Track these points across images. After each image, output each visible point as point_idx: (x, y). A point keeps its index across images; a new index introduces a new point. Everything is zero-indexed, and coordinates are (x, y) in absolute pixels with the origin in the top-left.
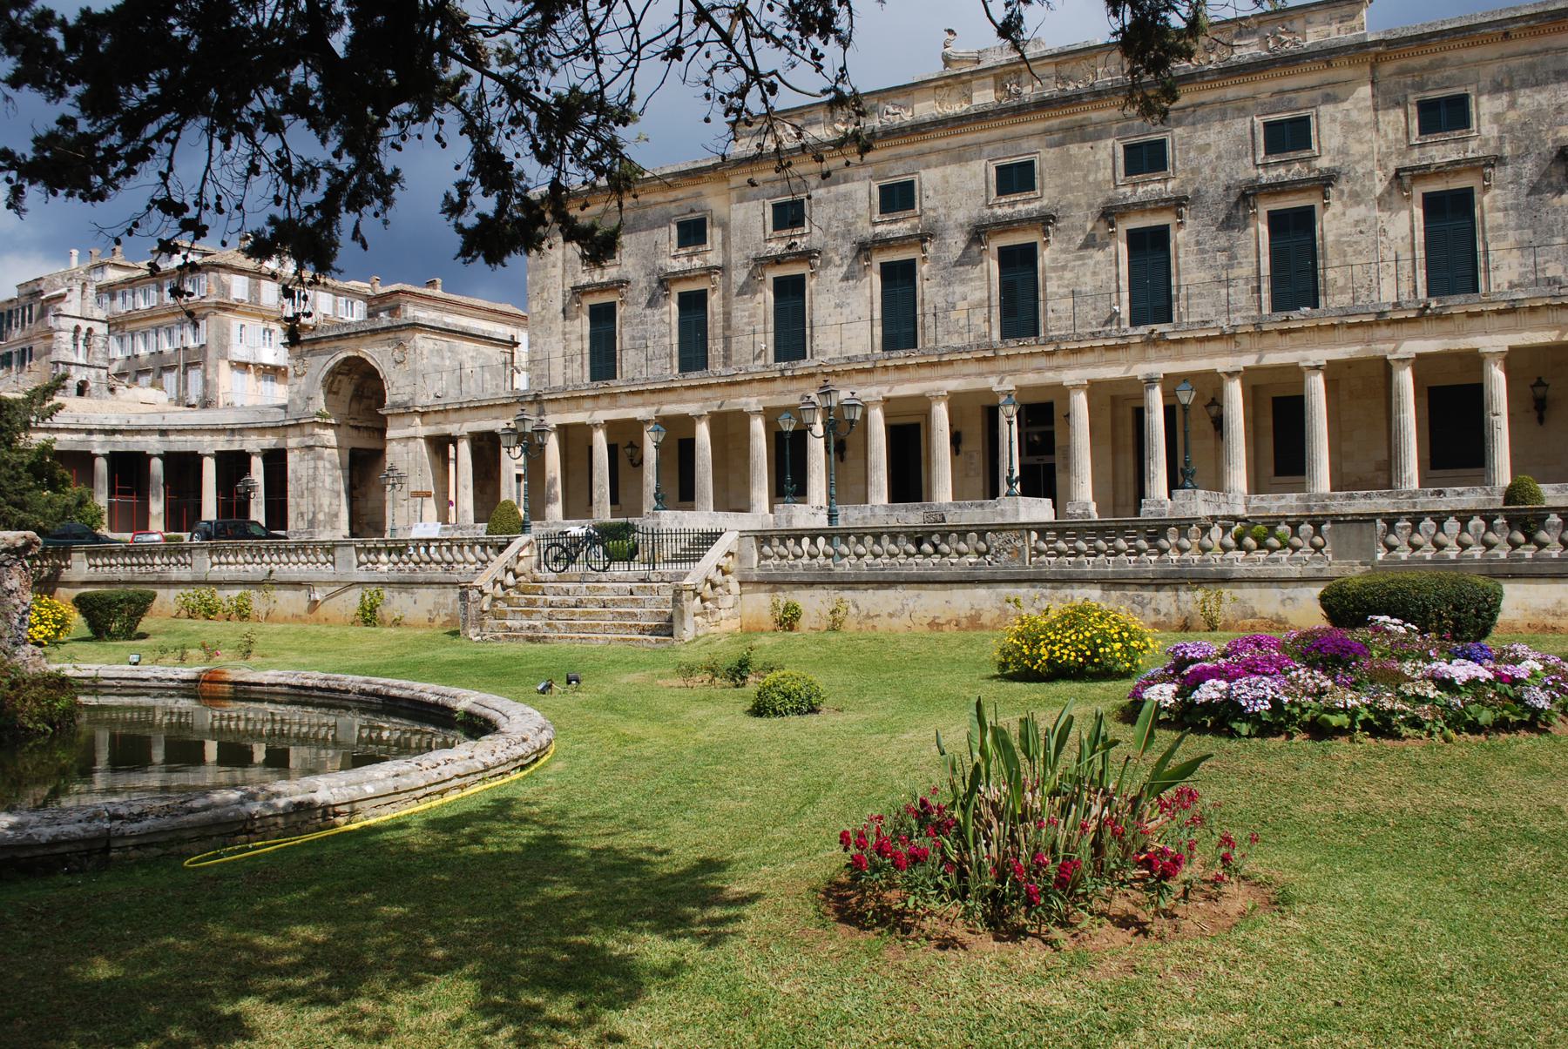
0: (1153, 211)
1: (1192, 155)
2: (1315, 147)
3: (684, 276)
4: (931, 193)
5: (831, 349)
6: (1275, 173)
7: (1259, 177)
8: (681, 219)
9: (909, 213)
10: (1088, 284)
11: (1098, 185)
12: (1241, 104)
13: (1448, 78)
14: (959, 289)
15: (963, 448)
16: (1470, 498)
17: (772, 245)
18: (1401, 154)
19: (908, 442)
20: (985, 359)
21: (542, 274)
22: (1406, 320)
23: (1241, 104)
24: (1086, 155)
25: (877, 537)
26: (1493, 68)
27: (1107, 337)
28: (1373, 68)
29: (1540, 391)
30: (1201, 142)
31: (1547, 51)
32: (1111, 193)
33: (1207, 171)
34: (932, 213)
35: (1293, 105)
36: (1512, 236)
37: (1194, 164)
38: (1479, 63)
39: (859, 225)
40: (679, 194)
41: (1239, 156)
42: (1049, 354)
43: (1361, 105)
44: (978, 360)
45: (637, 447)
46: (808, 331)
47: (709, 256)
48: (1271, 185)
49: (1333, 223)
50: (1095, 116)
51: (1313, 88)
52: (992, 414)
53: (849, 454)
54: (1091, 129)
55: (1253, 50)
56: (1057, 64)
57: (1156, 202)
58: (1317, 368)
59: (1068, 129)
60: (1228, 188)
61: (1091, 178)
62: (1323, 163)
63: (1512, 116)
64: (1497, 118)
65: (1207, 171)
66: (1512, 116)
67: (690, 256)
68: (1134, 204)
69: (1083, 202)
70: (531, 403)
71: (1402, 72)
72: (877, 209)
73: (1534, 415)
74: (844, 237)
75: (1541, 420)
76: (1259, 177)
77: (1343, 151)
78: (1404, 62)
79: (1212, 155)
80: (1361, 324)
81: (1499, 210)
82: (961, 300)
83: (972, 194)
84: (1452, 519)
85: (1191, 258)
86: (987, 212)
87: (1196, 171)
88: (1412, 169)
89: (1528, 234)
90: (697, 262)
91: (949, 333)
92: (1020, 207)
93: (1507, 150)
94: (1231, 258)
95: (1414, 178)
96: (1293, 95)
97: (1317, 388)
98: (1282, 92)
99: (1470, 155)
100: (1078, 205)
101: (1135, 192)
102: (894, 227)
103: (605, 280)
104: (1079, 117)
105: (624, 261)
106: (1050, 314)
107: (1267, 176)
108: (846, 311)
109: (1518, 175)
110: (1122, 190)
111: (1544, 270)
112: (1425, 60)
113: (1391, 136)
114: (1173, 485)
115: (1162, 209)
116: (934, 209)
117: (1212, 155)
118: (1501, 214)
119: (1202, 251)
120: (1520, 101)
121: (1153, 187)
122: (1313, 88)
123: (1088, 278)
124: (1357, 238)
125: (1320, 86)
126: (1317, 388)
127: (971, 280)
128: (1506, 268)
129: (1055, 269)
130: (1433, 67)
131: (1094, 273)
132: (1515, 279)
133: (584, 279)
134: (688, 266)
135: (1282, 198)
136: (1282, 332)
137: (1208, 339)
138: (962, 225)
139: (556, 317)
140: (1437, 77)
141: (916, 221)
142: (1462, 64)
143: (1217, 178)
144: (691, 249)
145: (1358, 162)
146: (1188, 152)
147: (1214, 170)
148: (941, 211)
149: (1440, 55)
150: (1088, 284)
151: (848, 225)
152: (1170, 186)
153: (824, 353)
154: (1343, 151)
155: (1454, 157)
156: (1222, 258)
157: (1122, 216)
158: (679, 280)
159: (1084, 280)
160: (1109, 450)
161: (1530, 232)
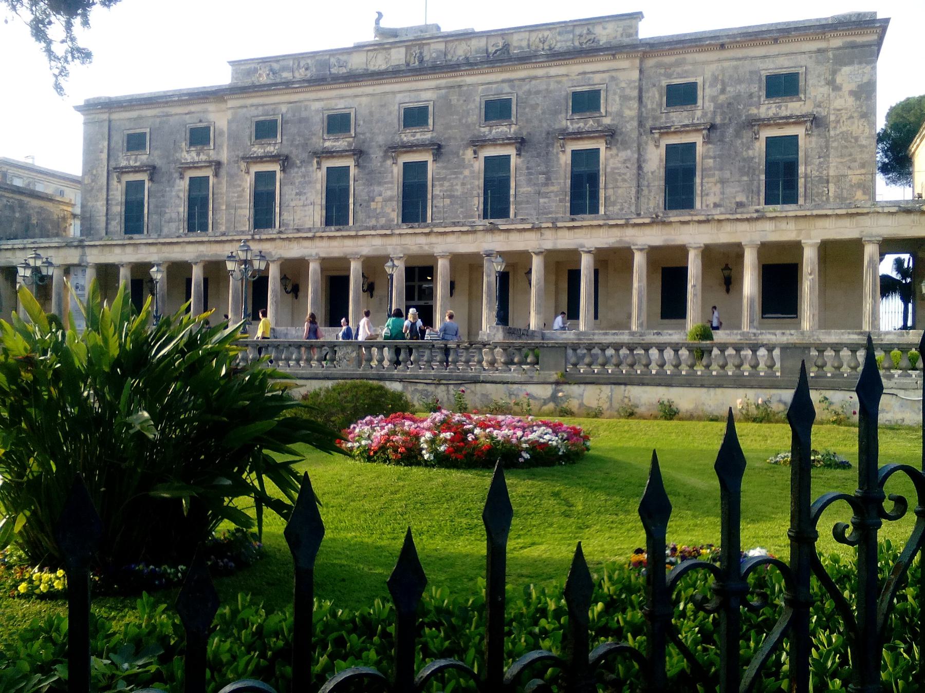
0: (501, 145)
1: (527, 110)
2: (603, 110)
3: (194, 166)
4: (361, 123)
6: (577, 126)
7: (567, 128)
8: (192, 126)
10: (459, 190)
11: (468, 126)
12: (559, 79)
13: (686, 71)
14: (377, 189)
16: (674, 336)
20: (386, 235)
22: (644, 224)
23: (559, 79)
26: (713, 67)
27: (463, 225)
28: (641, 62)
29: (727, 272)
30: (533, 102)
31: (745, 58)
32: (476, 132)
34: (362, 137)
35: (591, 82)
38: (704, 63)
39: (314, 139)
40: (193, 108)
41: (556, 113)
42: (426, 234)
43: (632, 85)
44: (381, 235)
46: (277, 210)
48: (574, 133)
50: (469, 80)
51: (604, 72)
54: (465, 88)
55: (569, 44)
56: (446, 42)
57: (503, 139)
58: (589, 252)
59: (452, 87)
60: (548, 133)
61: (464, 121)
62: (607, 121)
64: (713, 99)
65: (536, 123)
66: (722, 98)
68: (489, 140)
70: (76, 247)
71: (659, 65)
72: (326, 131)
73: (724, 288)
75: (728, 291)
77: (620, 114)
78: (660, 59)
79: (539, 111)
80: (617, 225)
81: (710, 158)
84: (668, 348)
86: (397, 139)
88: (661, 128)
90: (203, 157)
91: (369, 217)
93: (718, 120)
94: (548, 179)
95: (661, 134)
96: (591, 75)
98: (584, 73)
99: (696, 121)
100: (455, 139)
101: (490, 131)
103: (138, 164)
104: (458, 79)
106: (434, 209)
107: (572, 127)
108: (303, 198)
110: (483, 130)
111: (735, 198)
112: (672, 59)
113: (649, 107)
115: (508, 144)
116: (364, 134)
117: (539, 111)
118: (711, 161)
119: (530, 174)
120: (728, 89)
122: (604, 72)
123: (458, 187)
125: (607, 71)
127: (386, 183)
128: (712, 195)
129: (439, 179)
130: (678, 64)
131: (463, 184)
133: (123, 163)
134: (196, 159)
135: (581, 142)
136: (569, 228)
137: (524, 230)
139: (101, 189)
140: (679, 70)
141: (351, 139)
142: (695, 63)
145: (628, 122)
146: (524, 109)
147: (540, 121)
148: (368, 135)
149: (682, 56)
150: (459, 190)
152: (513, 128)
154: (620, 114)
155: (686, 122)
156: (542, 178)
157: (482, 146)
158: (190, 168)
160: (467, 299)
161: (728, 172)
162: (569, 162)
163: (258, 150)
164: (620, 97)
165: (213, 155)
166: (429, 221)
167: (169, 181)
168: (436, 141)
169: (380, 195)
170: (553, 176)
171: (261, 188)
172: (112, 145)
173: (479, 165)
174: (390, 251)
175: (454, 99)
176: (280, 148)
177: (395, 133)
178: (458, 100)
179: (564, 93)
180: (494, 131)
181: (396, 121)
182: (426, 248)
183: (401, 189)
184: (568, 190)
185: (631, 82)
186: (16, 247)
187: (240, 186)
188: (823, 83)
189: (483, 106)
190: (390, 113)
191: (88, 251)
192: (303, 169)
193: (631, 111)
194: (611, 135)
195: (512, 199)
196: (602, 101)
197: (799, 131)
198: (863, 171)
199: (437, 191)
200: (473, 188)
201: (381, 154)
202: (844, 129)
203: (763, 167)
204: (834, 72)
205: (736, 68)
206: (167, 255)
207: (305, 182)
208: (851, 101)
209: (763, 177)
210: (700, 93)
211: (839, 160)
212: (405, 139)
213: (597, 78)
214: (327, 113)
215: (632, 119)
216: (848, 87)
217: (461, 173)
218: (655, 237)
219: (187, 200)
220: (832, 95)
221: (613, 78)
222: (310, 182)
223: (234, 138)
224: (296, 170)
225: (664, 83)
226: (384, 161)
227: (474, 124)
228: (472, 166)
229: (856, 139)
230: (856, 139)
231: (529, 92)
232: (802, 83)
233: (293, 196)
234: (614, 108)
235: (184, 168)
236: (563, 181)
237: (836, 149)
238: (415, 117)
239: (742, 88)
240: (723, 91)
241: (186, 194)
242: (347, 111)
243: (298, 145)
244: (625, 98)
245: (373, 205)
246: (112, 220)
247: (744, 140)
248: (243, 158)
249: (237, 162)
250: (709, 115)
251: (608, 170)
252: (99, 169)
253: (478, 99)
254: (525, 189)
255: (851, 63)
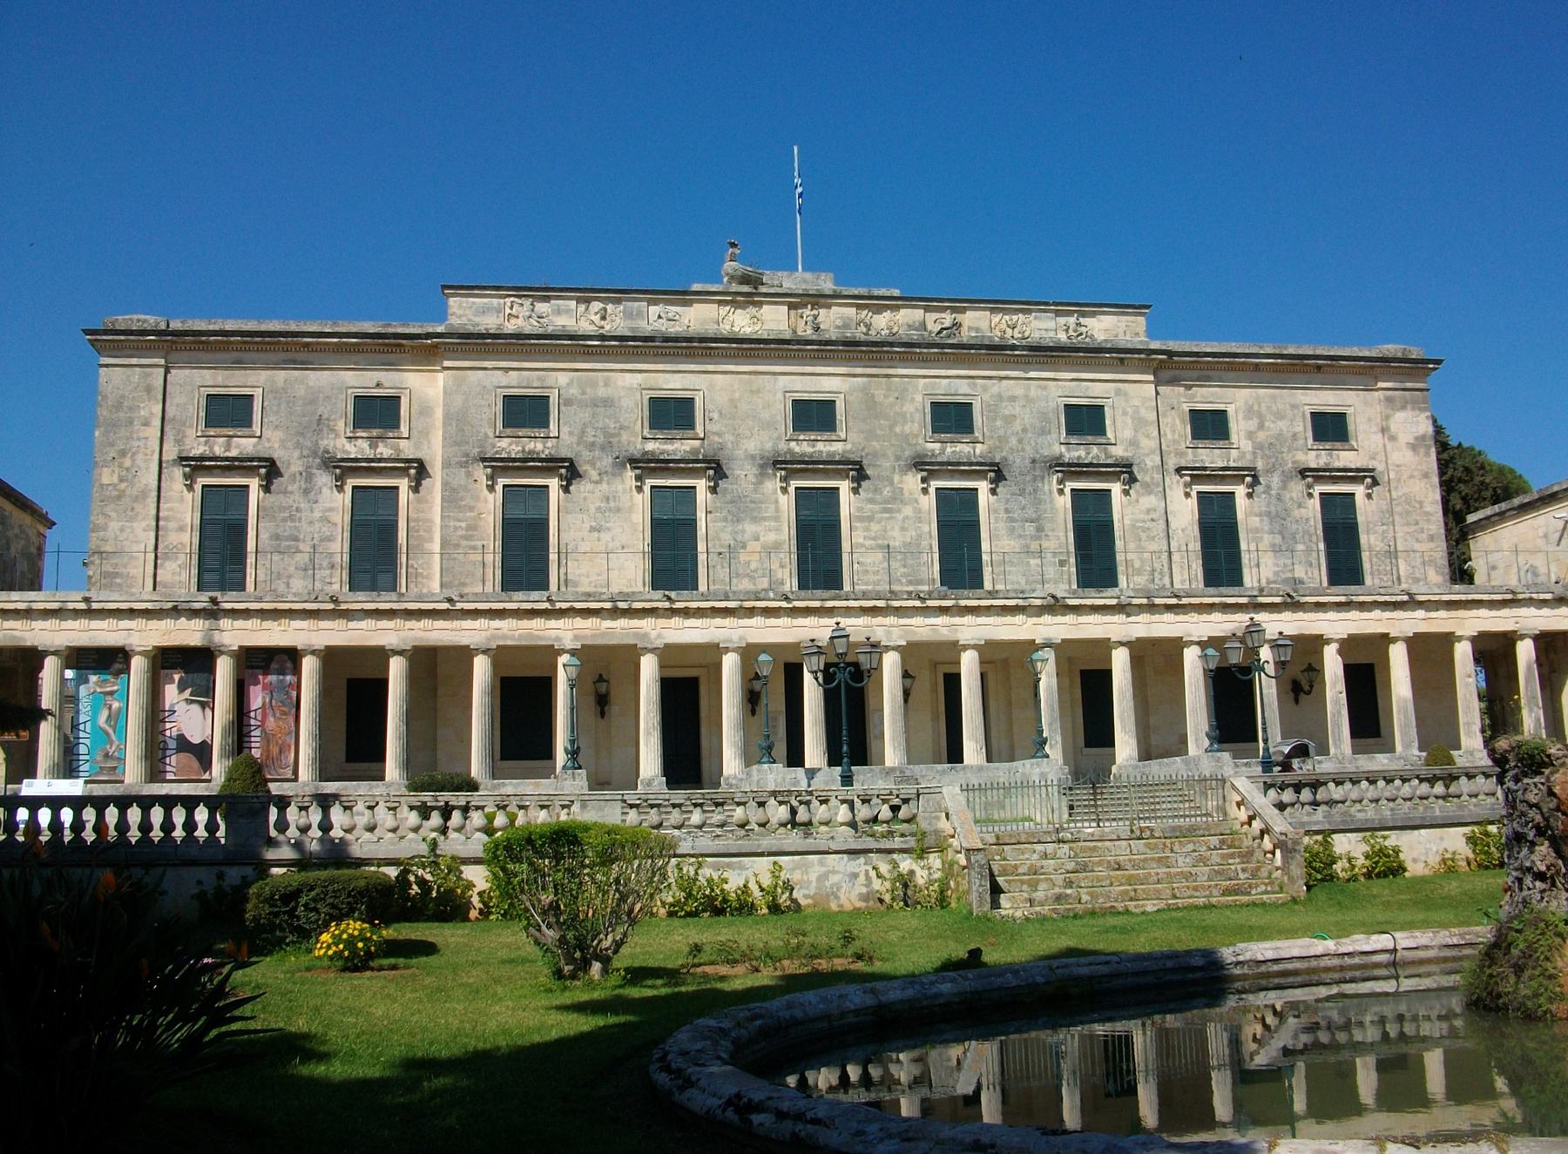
1: (998, 423)
2: (1110, 434)
4: (715, 416)
5: (585, 581)
6: (1076, 454)
7: (1061, 456)
9: (690, 433)
11: (905, 438)
14: (750, 528)
15: (761, 709)
17: (504, 443)
18: (1180, 454)
19: (685, 699)
21: (123, 432)
24: (892, 405)
25: (1389, 781)
33: (1014, 441)
34: (716, 439)
36: (1267, 539)
37: (1001, 432)
39: (625, 437)
41: (1044, 432)
45: (1314, 670)
47: (403, 444)
48: (1070, 465)
49: (1124, 507)
52: (793, 675)
53: (614, 709)
55: (1052, 334)
60: (1034, 461)
61: (898, 430)
62: (1118, 452)
63: (1261, 436)
65: (1014, 441)
66: (1261, 436)
67: (374, 442)
69: (890, 453)
72: (646, 424)
73: (1292, 695)
74: (603, 448)
76: (1061, 456)
77: (1134, 443)
79: (1017, 426)
82: (750, 535)
83: (769, 425)
85: (1001, 525)
86: (783, 446)
87: (1003, 439)
89: (1278, 539)
90: (384, 450)
92: (820, 446)
93: (1260, 465)
94: (1040, 529)
97: (1120, 663)
99: (1232, 464)
102: (669, 447)
103: (234, 453)
105: (267, 433)
107: (1071, 455)
108: (605, 537)
109: (1269, 487)
114: (1147, 753)
116: (719, 434)
117: (1017, 426)
119: (1012, 520)
121: (959, 449)
123: (896, 533)
124: (1149, 524)
126: (1120, 663)
127: (765, 519)
129: (860, 519)
131: (903, 529)
132: (1271, 576)
133: (199, 450)
134: (369, 453)
136: (1169, 608)
138: (753, 457)
141: (697, 443)
143: (1023, 450)
144: (375, 433)
146: (994, 420)
147: (1020, 441)
148: (728, 437)
150: (897, 539)
151: (607, 435)
153: (576, 584)
154: (1134, 443)
156: (1030, 528)
159: (888, 531)
162: (1069, 505)
163: (510, 447)
164: (1133, 418)
165: (408, 449)
166: (988, 585)
167: (306, 492)
168: (853, 457)
169: (757, 539)
170: (1048, 526)
171: (518, 513)
172: (170, 412)
173: (929, 503)
174: (879, 635)
175: (879, 394)
176: (557, 446)
177: (779, 438)
178: (886, 396)
179: (1052, 405)
180: (949, 450)
181: (780, 418)
182: (945, 631)
183: (793, 532)
184: (1072, 549)
185: (1145, 400)
186: (35, 606)
187: (471, 509)
188: (1374, 429)
189: (928, 410)
190: (768, 406)
191: (225, 623)
192: (604, 486)
193: (1148, 444)
194: (1125, 471)
195: (985, 557)
196: (1108, 422)
197: (1359, 491)
198: (1432, 545)
199: (858, 537)
200: (920, 536)
201: (755, 471)
202: (1406, 490)
203: (1320, 532)
204: (1387, 417)
205: (1273, 398)
206: (421, 634)
207: (610, 510)
208: (1409, 454)
209: (1322, 546)
210: (1233, 426)
211: (1406, 529)
212: (797, 449)
213: (1098, 389)
214: (647, 395)
215: (1153, 452)
216: (1406, 437)
217: (899, 511)
218: (925, 628)
219: (347, 528)
220: (1389, 446)
221: (1118, 392)
222: (618, 510)
223: (457, 420)
224: (590, 487)
225: (1231, 409)
226: (760, 483)
227: (916, 436)
228: (916, 501)
229: (1421, 503)
230: (1421, 503)
231: (1000, 396)
232: (1351, 427)
233: (586, 533)
234: (1127, 434)
235: (343, 469)
236: (1061, 536)
237: (1400, 514)
238: (814, 415)
239: (1282, 425)
240: (1261, 426)
241: (347, 518)
242: (687, 394)
243: (593, 444)
244: (1139, 423)
245: (743, 558)
246: (167, 557)
247: (1294, 495)
248: (484, 460)
249: (464, 465)
250: (1249, 457)
251: (1127, 522)
252: (140, 457)
253: (919, 398)
254: (1008, 544)
255: (1403, 408)
